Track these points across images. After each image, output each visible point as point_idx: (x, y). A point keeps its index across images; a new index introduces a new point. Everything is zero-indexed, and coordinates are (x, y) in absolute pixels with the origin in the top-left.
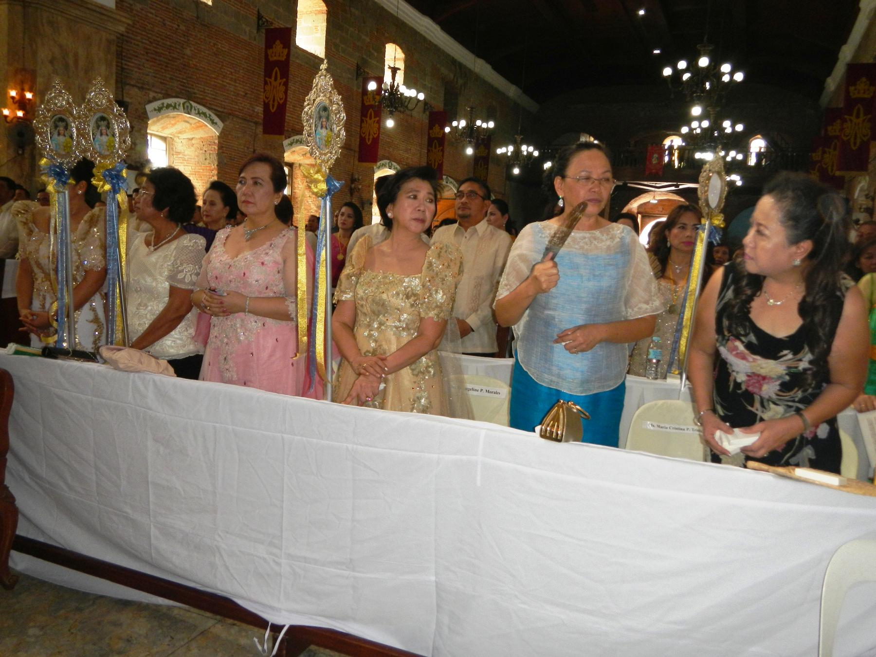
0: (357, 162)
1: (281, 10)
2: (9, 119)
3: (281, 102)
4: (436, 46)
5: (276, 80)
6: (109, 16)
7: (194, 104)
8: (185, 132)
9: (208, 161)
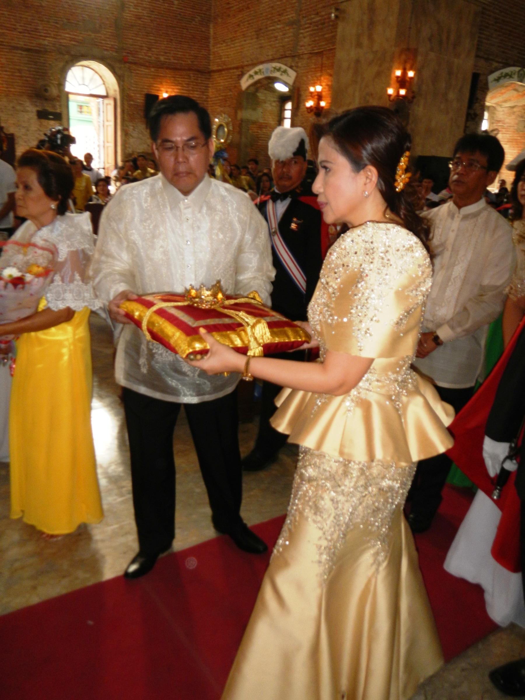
8: (510, 100)
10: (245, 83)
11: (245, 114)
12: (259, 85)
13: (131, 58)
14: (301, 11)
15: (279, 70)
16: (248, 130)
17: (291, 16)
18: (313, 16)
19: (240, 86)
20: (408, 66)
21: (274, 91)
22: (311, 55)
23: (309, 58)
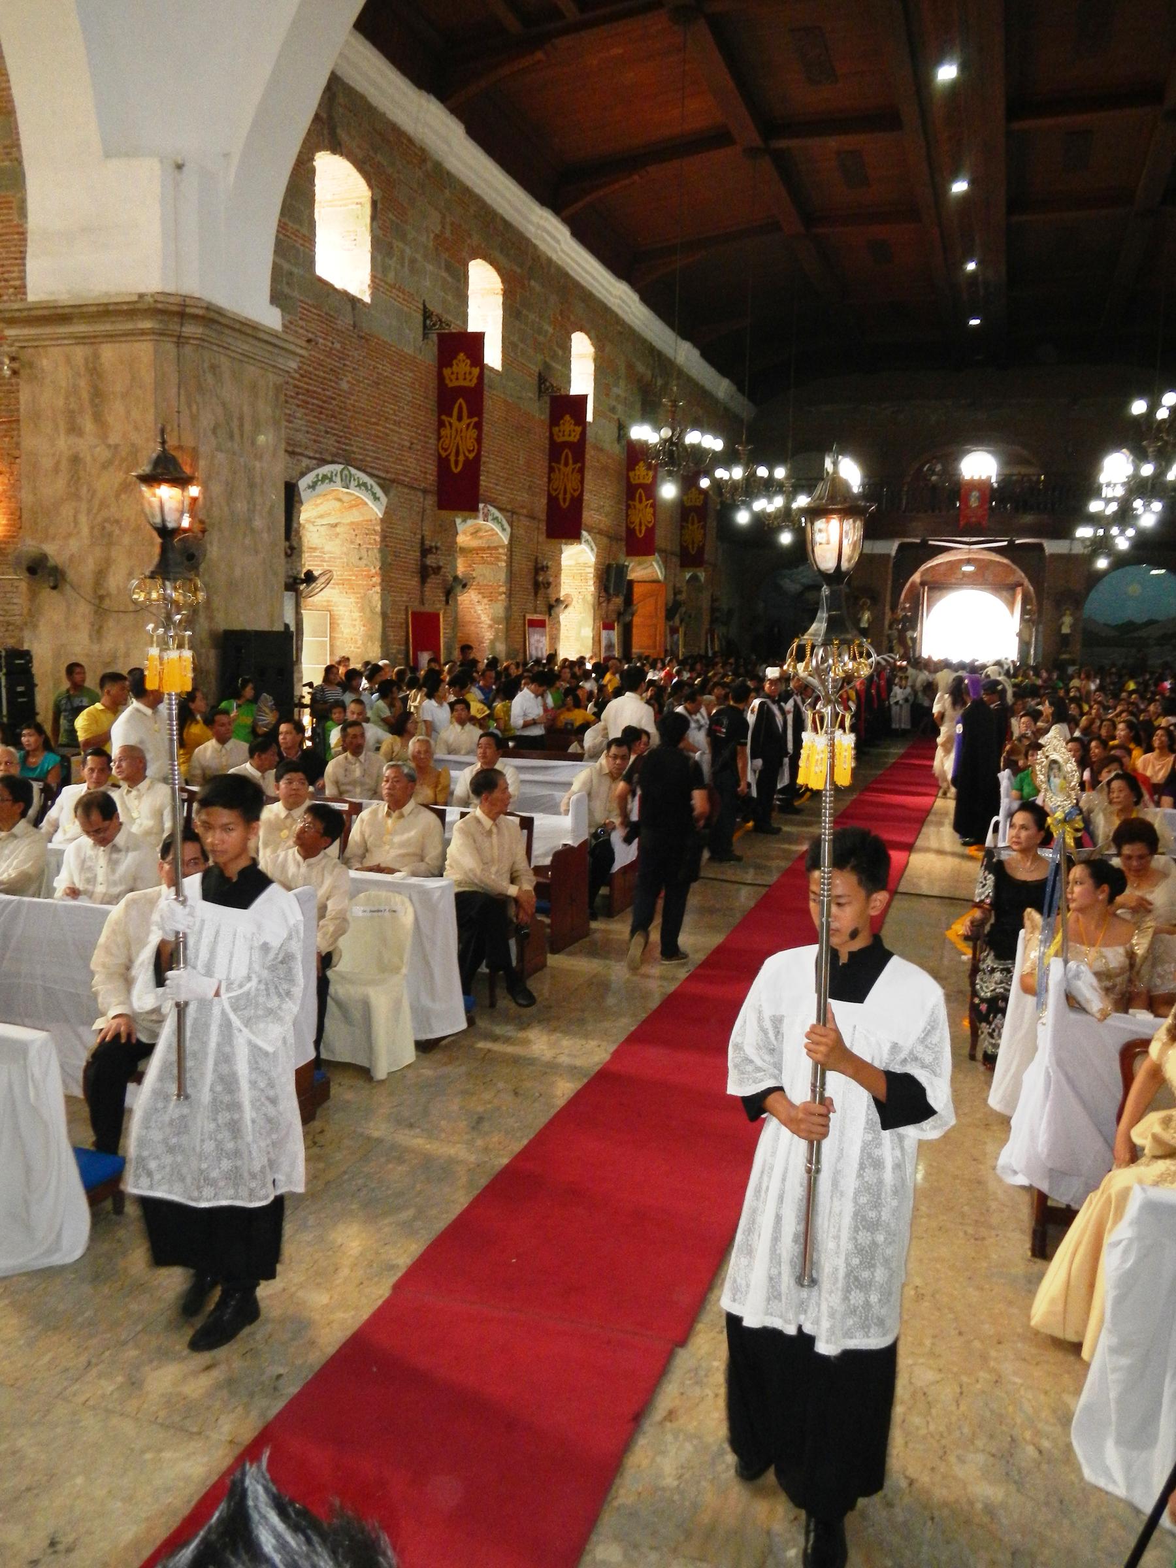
0: (542, 538)
1: (450, 298)
3: (471, 456)
4: (630, 327)
5: (460, 419)
6: (282, 348)
7: (353, 471)
9: (364, 562)
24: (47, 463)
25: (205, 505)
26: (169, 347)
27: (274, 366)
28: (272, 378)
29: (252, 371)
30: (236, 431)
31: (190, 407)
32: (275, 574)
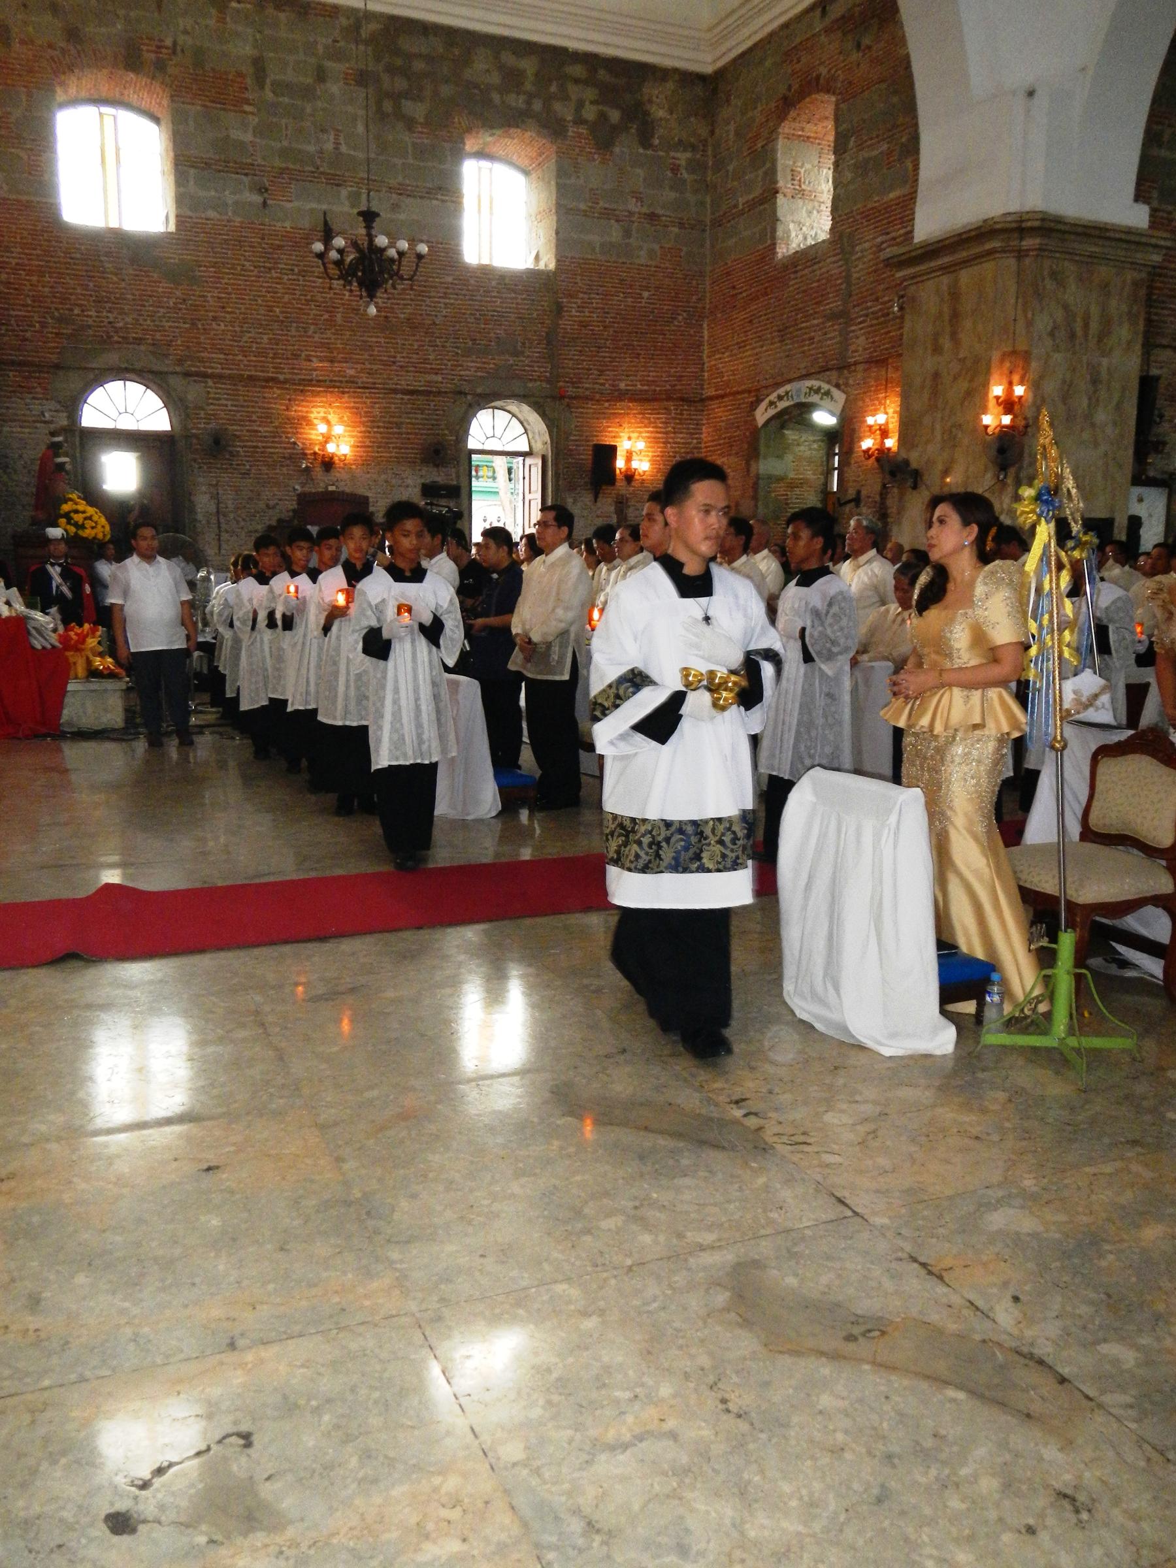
2: (990, 431)
10: (762, 415)
11: (767, 466)
12: (786, 417)
13: (571, 391)
14: (850, 296)
15: (818, 391)
16: (769, 492)
17: (834, 304)
18: (869, 304)
19: (755, 419)
20: (1016, 378)
21: (811, 426)
22: (867, 366)
23: (865, 370)
24: (918, 381)
25: (1034, 403)
26: (1012, 262)
27: (1132, 263)
28: (1130, 276)
29: (1104, 271)
30: (1079, 332)
31: (1025, 311)
32: (1120, 466)
